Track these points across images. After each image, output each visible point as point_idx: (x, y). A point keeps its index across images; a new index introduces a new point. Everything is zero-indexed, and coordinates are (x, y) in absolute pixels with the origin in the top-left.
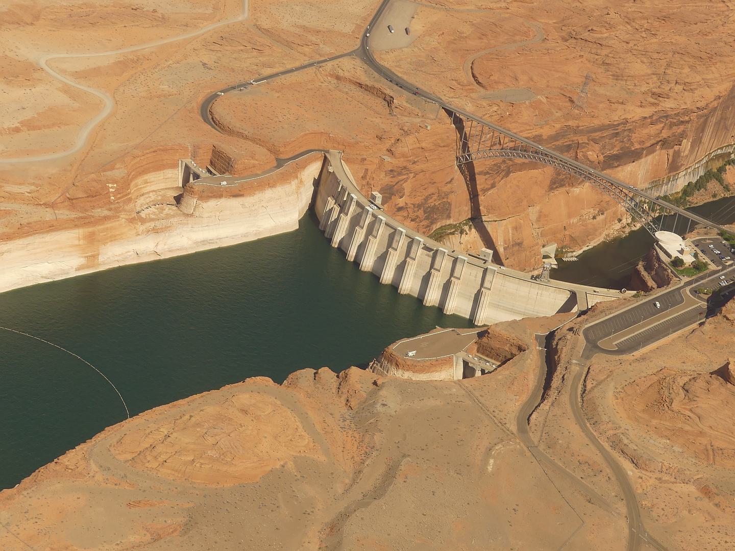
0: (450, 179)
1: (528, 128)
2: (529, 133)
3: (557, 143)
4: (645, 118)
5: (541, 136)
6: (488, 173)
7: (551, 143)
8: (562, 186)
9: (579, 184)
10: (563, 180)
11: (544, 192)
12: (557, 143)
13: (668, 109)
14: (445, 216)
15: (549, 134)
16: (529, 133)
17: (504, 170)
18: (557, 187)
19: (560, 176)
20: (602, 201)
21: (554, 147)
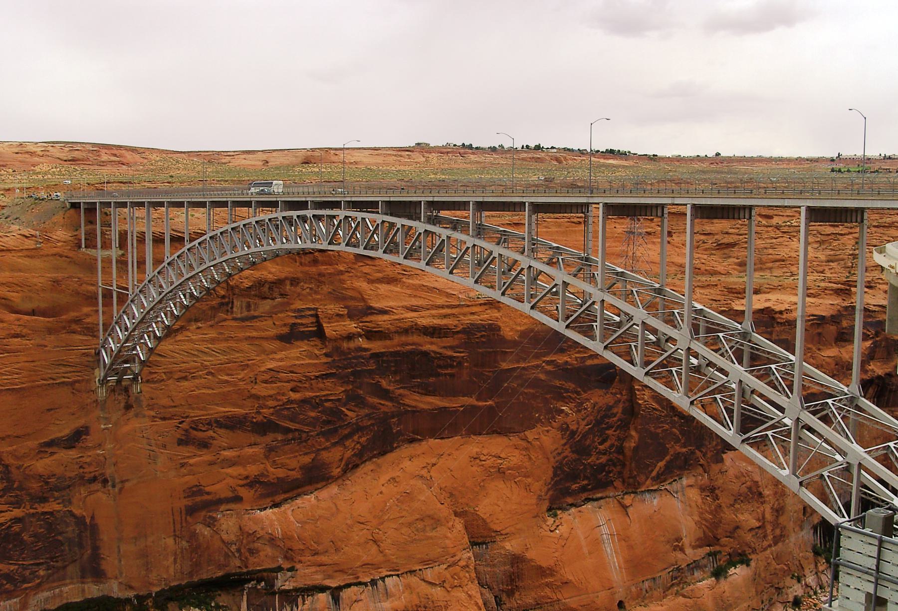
0: (67, 432)
1: (441, 301)
2: (445, 316)
3: (561, 359)
4: (822, 318)
5: (493, 329)
6: (264, 428)
7: (537, 356)
8: (604, 485)
9: (660, 478)
10: (602, 468)
11: (534, 501)
12: (561, 359)
13: (877, 309)
14: (73, 570)
15: (522, 328)
16: (445, 316)
17: (358, 429)
18: (584, 489)
19: (590, 455)
20: (737, 527)
21: (549, 368)
